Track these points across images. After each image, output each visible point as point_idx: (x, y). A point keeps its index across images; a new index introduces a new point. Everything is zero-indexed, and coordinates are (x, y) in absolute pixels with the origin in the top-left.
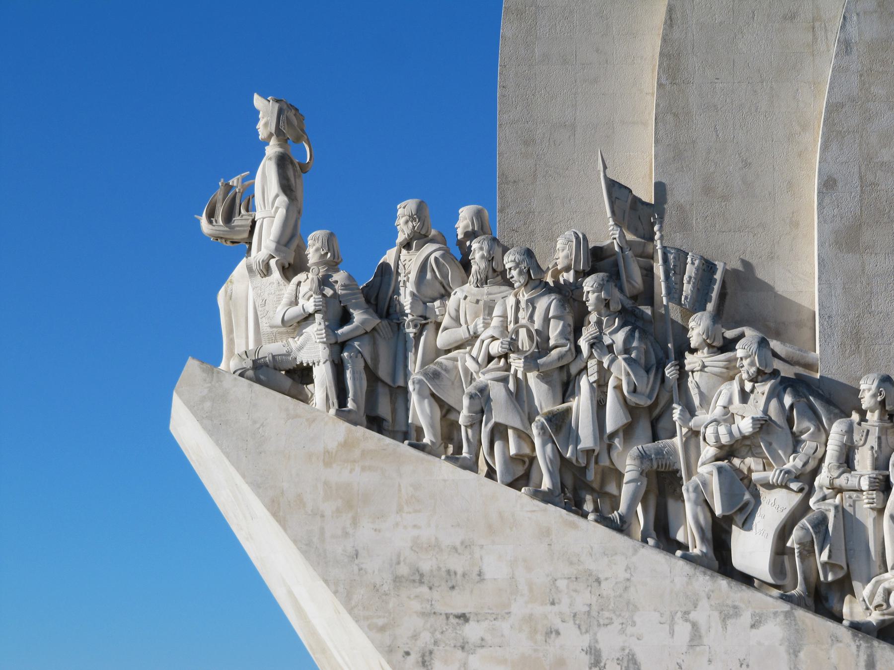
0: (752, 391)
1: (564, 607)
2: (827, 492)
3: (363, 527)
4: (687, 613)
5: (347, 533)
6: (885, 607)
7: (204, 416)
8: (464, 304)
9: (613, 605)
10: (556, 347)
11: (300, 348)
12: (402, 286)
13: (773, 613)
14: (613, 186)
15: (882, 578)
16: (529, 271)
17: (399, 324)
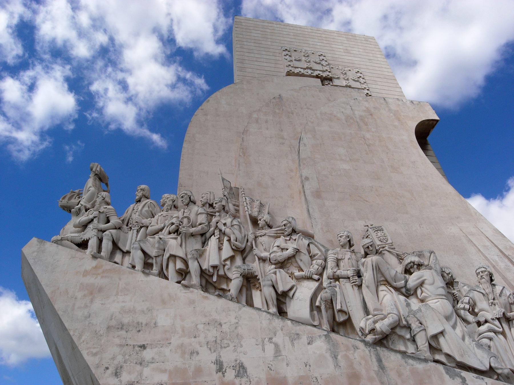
0: (290, 240)
1: (202, 339)
2: (331, 280)
3: (96, 303)
4: (271, 339)
5: (87, 306)
6: (375, 331)
7: (32, 258)
8: (160, 218)
9: (229, 337)
10: (200, 224)
11: (84, 234)
12: (134, 214)
13: (319, 336)
14: (223, 179)
15: (368, 318)
16: (190, 198)
17: (131, 228)
